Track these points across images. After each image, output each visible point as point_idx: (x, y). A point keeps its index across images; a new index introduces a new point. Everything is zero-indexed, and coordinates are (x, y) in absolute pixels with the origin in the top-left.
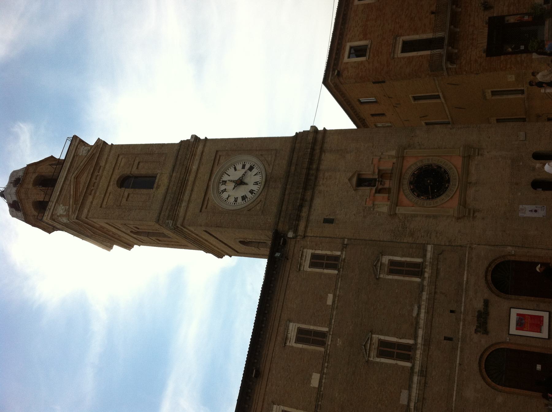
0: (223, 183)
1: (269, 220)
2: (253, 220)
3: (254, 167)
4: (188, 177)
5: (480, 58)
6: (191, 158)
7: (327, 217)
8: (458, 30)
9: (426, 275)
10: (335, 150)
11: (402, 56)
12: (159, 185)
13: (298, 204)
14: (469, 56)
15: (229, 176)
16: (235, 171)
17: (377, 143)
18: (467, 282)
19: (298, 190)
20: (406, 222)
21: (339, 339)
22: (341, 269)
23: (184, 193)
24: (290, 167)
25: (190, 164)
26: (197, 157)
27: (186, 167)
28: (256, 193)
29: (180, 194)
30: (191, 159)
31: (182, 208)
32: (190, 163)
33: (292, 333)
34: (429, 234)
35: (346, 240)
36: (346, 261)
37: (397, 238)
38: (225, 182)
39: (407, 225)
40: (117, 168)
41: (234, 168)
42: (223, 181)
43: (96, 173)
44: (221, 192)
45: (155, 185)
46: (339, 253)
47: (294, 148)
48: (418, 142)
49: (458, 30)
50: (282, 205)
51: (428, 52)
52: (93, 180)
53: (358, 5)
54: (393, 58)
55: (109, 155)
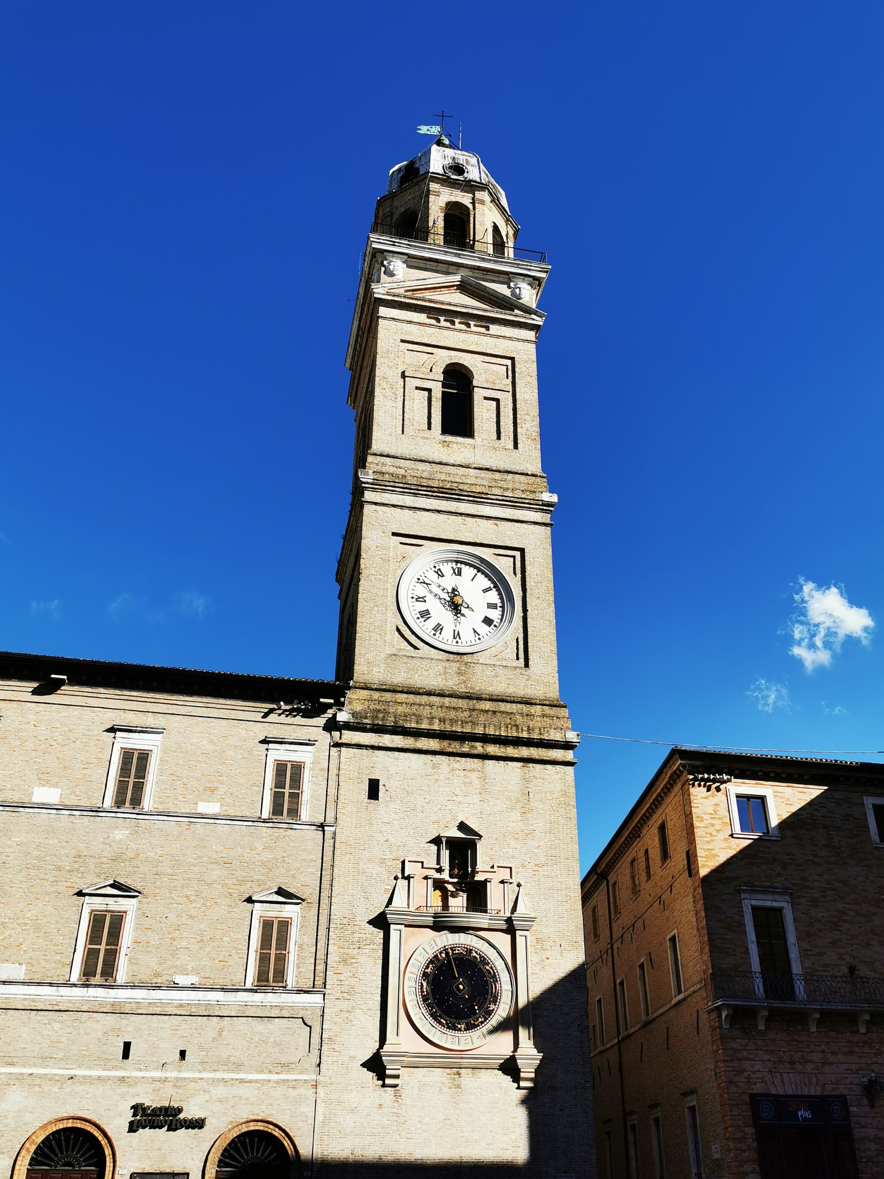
0: (456, 571)
1: (375, 669)
2: (375, 638)
3: (492, 626)
4: (465, 500)
7: (380, 787)
8: (813, 1029)
9: (258, 997)
10: (528, 787)
11: (745, 908)
12: (451, 446)
13: (408, 725)
14: (751, 1056)
15: (472, 580)
16: (483, 591)
17: (546, 873)
18: (242, 1081)
19: (437, 720)
20: (371, 947)
21: (128, 832)
22: (271, 825)
23: (432, 496)
24: (491, 700)
28: (434, 637)
29: (429, 489)
32: (497, 500)
33: (137, 742)
34: (345, 995)
35: (333, 829)
37: (336, 931)
38: (459, 574)
39: (365, 949)
41: (490, 587)
42: (460, 571)
44: (438, 568)
45: (449, 438)
46: (305, 814)
47: (531, 704)
49: (813, 1029)
50: (406, 693)
51: (756, 965)
53: (863, 804)
54: (739, 892)
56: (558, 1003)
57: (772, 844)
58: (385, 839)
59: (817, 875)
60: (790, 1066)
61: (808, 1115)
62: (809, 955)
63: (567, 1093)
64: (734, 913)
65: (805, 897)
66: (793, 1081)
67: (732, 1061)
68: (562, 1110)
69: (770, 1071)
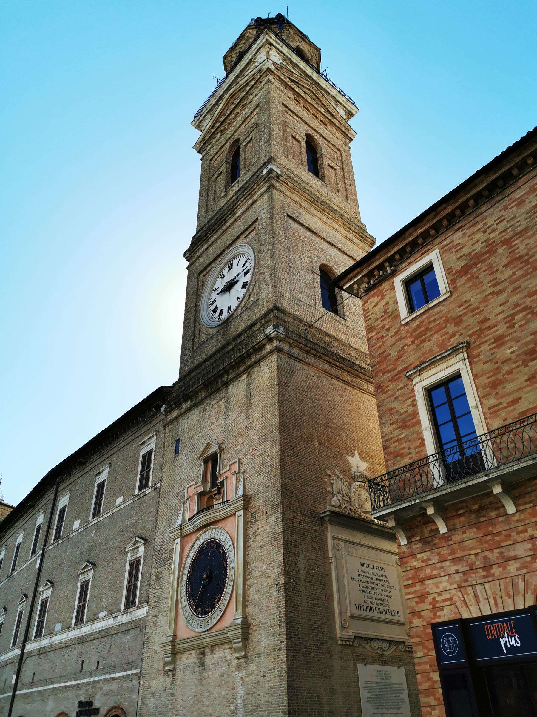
5: (431, 607)
6: (247, 197)
8: (511, 509)
14: (435, 572)
25: (240, 204)
26: (250, 202)
27: (236, 204)
30: (245, 198)
31: (202, 249)
32: (242, 202)
36: (146, 498)
40: (247, 122)
43: (238, 110)
48: (258, 529)
49: (511, 509)
52: (233, 115)
54: (409, 378)
55: (256, 95)
56: (263, 568)
57: (443, 306)
58: (179, 478)
59: (500, 306)
60: (484, 573)
61: (515, 641)
62: (499, 411)
63: (268, 657)
64: (408, 406)
65: (486, 342)
66: (489, 593)
67: (413, 585)
68: (264, 676)
69: (460, 587)
